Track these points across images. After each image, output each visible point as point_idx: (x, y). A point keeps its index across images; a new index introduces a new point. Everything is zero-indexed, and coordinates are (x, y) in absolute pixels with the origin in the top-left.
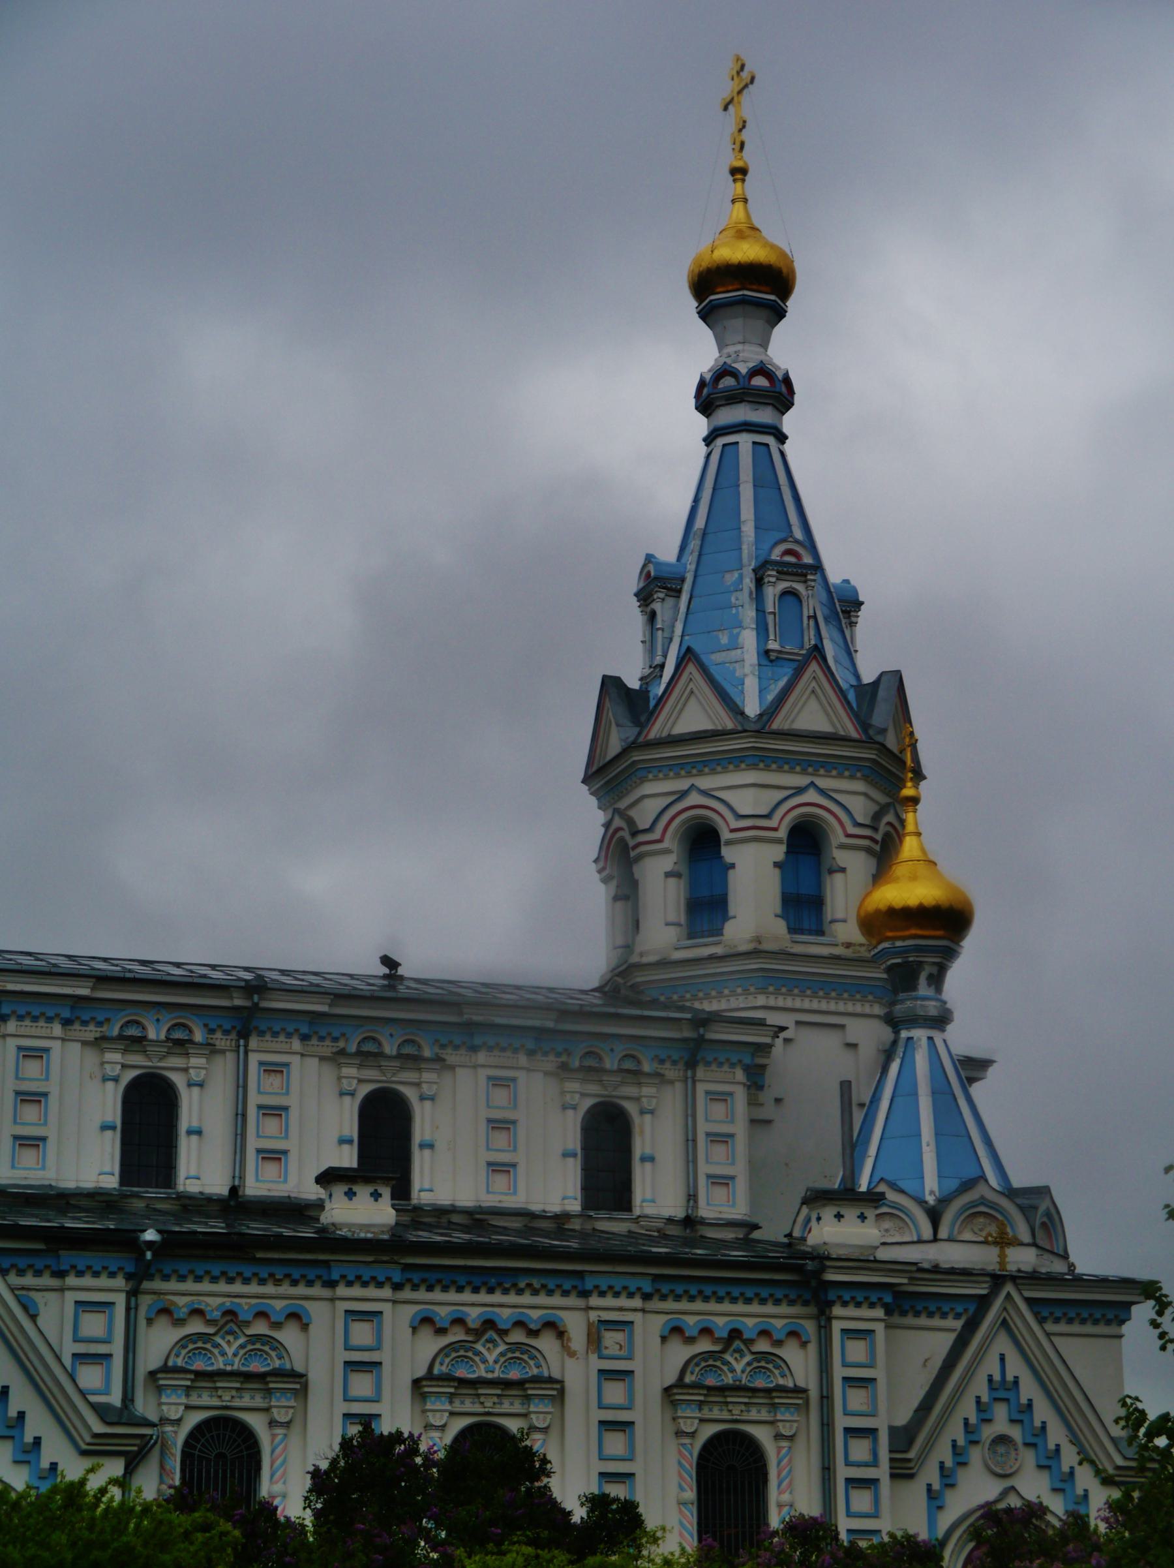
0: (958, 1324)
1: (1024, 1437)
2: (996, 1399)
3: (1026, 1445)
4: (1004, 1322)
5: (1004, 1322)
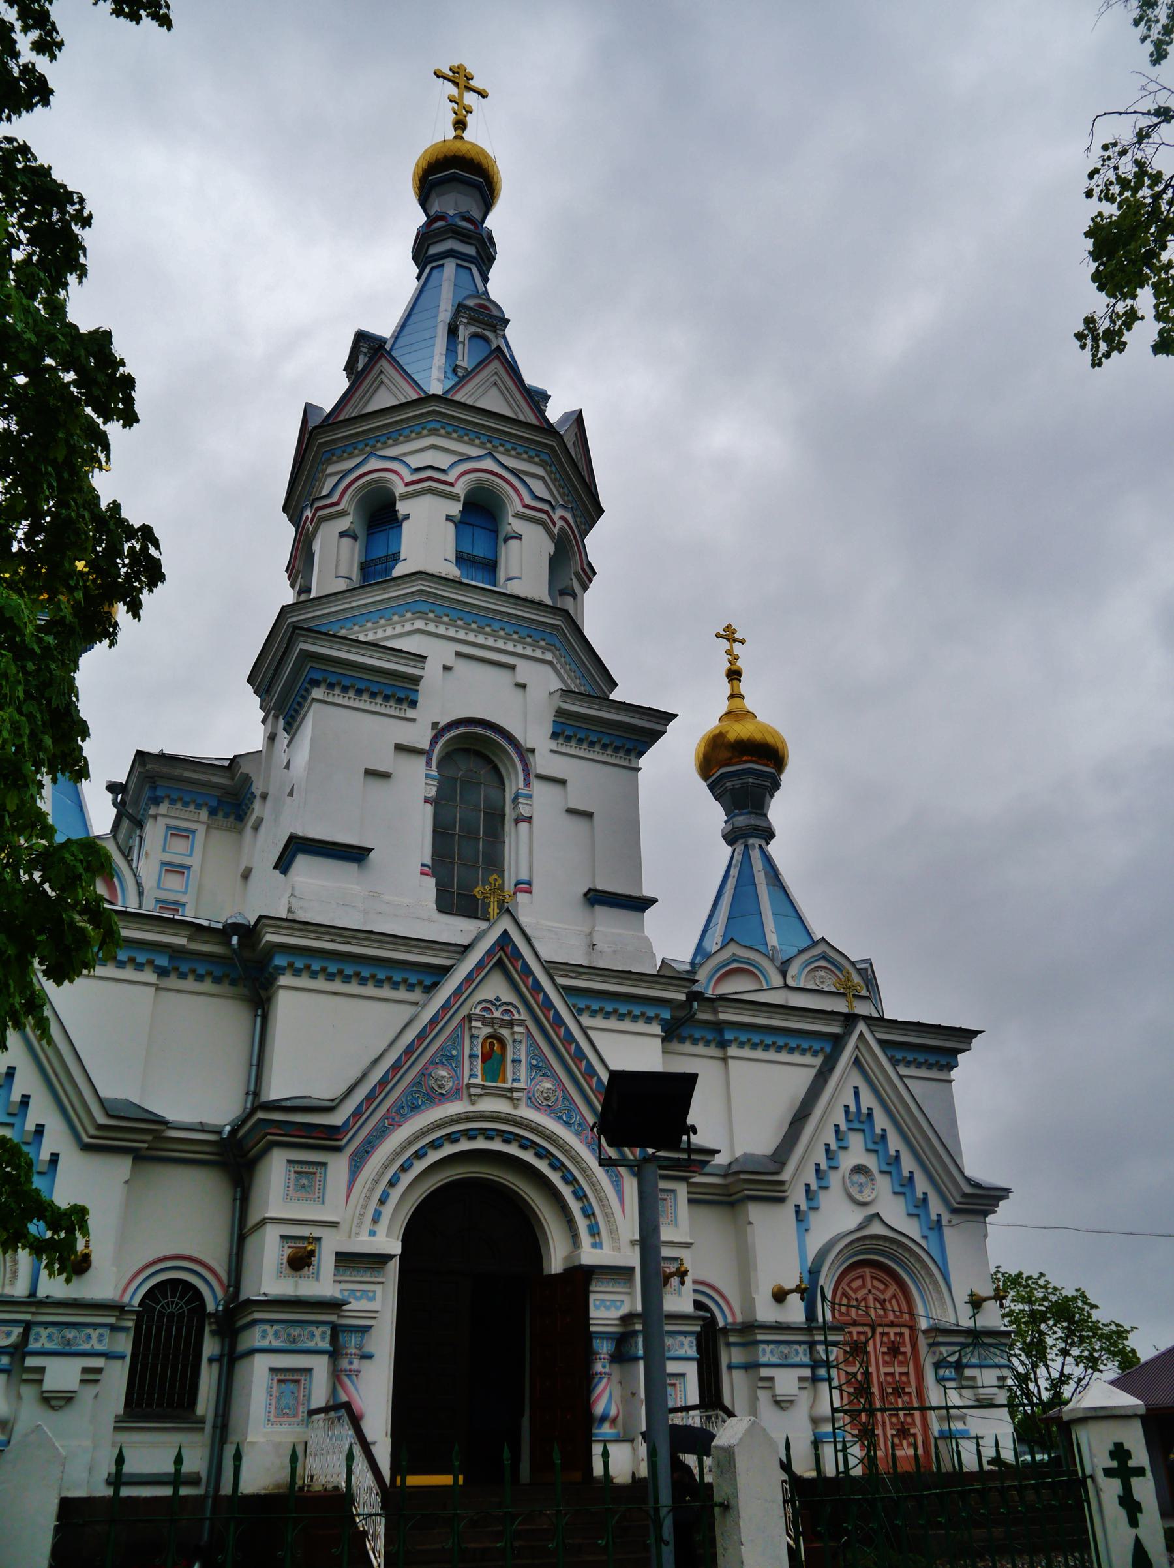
0: (818, 1061)
1: (879, 1166)
2: (850, 1129)
3: (882, 1172)
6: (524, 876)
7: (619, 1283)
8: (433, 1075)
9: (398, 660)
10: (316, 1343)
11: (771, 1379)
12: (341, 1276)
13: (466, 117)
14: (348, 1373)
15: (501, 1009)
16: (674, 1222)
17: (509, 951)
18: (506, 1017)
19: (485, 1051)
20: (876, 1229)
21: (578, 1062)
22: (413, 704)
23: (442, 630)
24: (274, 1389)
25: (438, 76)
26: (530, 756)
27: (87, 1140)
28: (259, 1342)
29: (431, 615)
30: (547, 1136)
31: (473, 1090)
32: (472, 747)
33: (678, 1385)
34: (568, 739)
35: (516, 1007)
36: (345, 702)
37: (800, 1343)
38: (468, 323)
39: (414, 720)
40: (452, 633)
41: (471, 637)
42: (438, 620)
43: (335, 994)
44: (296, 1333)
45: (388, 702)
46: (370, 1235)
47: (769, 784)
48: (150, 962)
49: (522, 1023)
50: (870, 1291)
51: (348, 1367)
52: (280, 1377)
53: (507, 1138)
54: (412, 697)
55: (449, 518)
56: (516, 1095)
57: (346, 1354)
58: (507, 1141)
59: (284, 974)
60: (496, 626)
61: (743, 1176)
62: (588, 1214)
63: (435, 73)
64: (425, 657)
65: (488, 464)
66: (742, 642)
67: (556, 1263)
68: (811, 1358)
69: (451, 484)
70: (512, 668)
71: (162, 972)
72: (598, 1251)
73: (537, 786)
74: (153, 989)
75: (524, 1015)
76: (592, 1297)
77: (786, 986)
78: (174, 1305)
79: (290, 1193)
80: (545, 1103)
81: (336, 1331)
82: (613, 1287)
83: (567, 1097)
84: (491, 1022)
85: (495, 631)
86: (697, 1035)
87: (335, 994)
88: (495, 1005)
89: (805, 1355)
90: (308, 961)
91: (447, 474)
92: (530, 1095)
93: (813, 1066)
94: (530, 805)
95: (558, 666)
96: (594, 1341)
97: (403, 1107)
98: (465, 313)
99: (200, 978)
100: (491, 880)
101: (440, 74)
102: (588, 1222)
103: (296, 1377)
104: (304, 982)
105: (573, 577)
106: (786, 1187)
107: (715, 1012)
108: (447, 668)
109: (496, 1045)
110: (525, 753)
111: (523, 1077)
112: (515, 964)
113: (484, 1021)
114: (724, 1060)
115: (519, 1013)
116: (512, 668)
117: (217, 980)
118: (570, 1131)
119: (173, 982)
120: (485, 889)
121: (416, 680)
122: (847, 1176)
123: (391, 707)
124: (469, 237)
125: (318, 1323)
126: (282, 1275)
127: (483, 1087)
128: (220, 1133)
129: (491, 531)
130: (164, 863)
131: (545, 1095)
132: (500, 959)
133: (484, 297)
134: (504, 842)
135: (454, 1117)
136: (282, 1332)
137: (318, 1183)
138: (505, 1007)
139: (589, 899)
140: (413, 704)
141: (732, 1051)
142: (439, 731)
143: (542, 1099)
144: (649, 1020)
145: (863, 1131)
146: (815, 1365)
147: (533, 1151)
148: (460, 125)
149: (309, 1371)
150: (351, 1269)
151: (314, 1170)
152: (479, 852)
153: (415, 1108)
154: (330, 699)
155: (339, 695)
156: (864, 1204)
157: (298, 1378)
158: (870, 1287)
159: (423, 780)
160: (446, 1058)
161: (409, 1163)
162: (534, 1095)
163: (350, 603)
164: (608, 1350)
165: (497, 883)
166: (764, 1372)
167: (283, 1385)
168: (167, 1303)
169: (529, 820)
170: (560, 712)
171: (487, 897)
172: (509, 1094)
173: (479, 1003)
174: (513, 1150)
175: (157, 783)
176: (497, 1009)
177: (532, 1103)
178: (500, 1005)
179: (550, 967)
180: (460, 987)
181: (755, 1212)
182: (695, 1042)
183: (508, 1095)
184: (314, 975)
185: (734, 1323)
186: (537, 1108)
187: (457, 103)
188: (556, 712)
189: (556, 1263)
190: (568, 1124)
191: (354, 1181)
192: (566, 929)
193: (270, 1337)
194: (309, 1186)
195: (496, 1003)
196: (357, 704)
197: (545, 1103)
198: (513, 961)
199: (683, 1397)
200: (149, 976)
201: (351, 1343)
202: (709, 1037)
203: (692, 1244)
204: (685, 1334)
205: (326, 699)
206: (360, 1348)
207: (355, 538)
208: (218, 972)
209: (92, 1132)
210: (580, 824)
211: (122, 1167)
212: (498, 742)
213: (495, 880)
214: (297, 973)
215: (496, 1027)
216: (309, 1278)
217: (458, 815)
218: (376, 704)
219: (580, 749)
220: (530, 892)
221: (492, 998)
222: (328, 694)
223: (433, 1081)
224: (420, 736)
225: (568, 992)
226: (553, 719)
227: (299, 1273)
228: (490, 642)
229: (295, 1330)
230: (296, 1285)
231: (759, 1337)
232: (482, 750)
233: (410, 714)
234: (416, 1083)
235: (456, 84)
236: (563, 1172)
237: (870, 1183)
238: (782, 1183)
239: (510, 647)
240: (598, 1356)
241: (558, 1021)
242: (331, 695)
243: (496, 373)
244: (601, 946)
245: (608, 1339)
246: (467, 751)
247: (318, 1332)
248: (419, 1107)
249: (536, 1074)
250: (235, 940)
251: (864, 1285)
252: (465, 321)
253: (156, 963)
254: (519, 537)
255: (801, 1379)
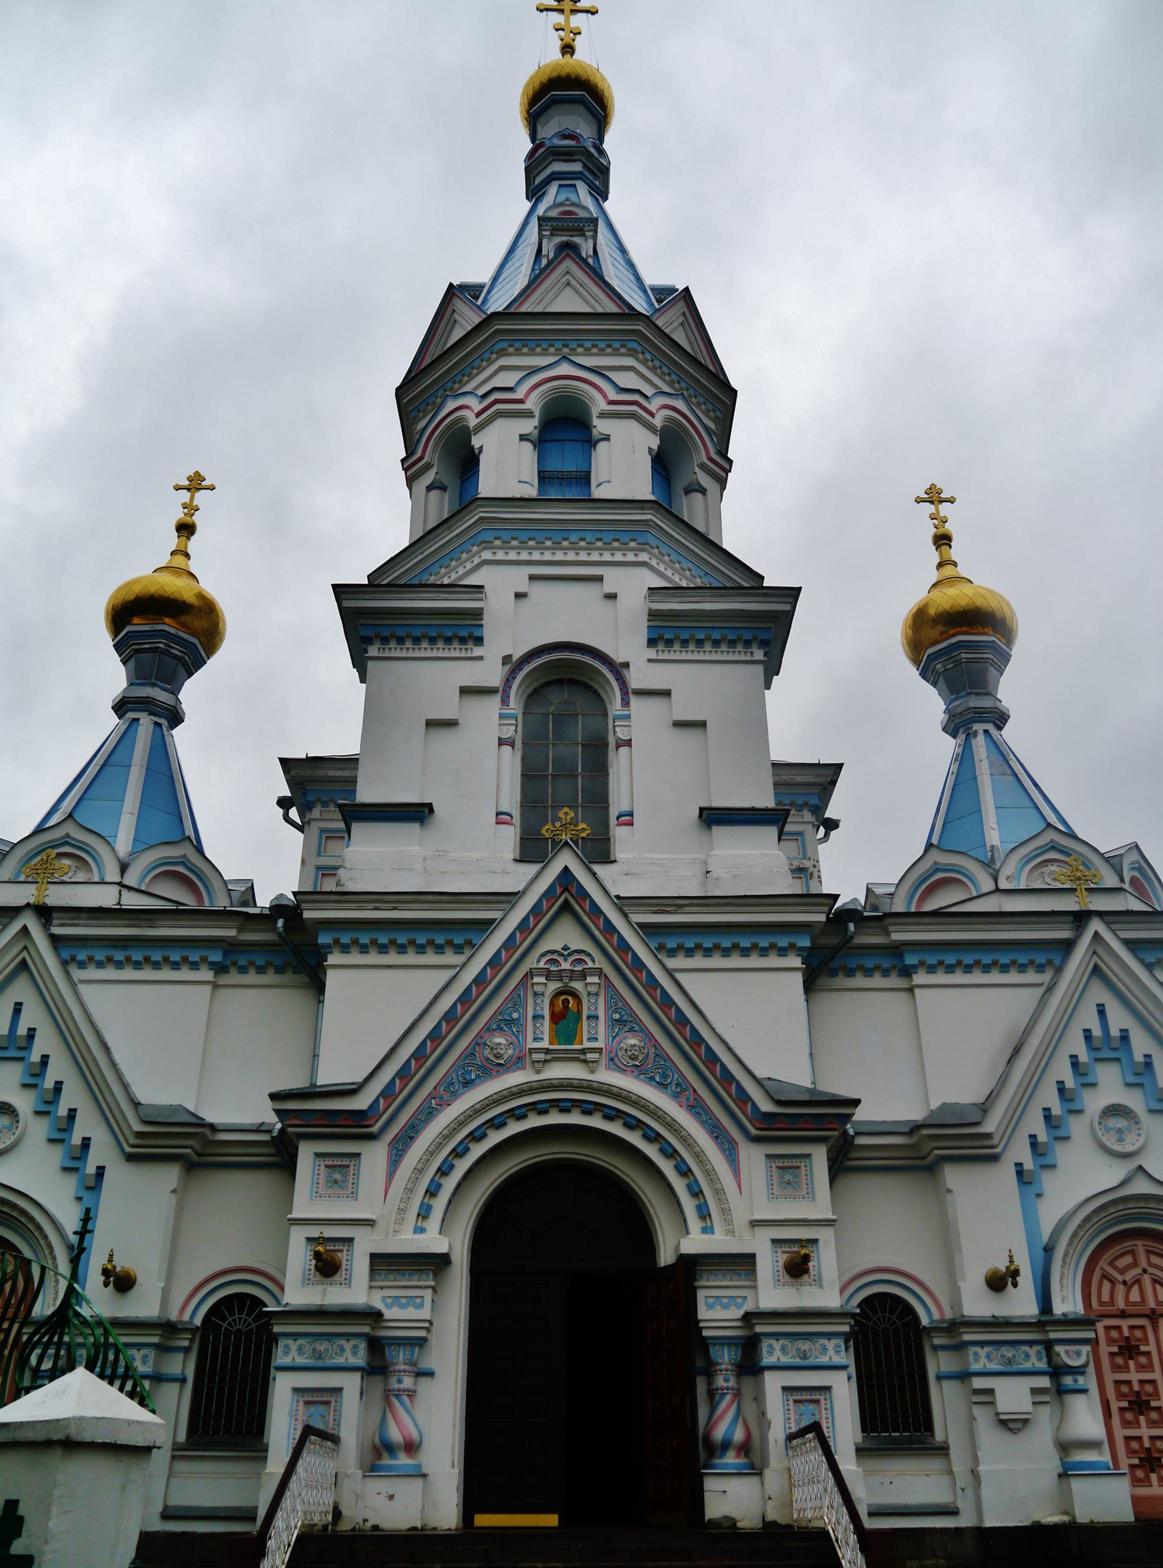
3: (1151, 1111)
4: (1096, 970)
5: (1096, 970)
6: (625, 807)
7: (739, 1275)
8: (489, 1043)
9: (451, 596)
10: (347, 1358)
11: (991, 1392)
12: (383, 1280)
13: (574, 40)
14: (396, 1393)
15: (571, 959)
16: (810, 1195)
17: (574, 891)
18: (579, 968)
19: (557, 1010)
20: (1141, 1187)
21: (666, 1010)
22: (479, 641)
23: (512, 556)
24: (300, 1413)
25: (541, 11)
26: (625, 671)
27: (128, 1149)
28: (281, 1358)
29: (498, 542)
30: (633, 1102)
31: (535, 1056)
32: (566, 677)
33: (823, 1402)
34: (669, 643)
35: (589, 955)
36: (404, 654)
37: (1030, 1343)
38: (552, 235)
39: (481, 658)
40: (524, 556)
41: (548, 556)
42: (506, 547)
43: (389, 967)
44: (322, 1348)
45: (451, 645)
46: (415, 1232)
47: (991, 656)
48: (204, 959)
49: (600, 972)
50: (1145, 1271)
51: (396, 1386)
52: (306, 1399)
53: (589, 1109)
54: (477, 633)
55: (523, 438)
56: (590, 1056)
57: (395, 1371)
58: (587, 1113)
59: (331, 952)
60: (574, 537)
61: (925, 1132)
62: (696, 1193)
63: (538, 9)
64: (482, 587)
65: (565, 369)
66: (951, 501)
67: (666, 1257)
68: (1050, 1363)
69: (521, 401)
70: (599, 579)
71: (220, 969)
72: (707, 1237)
73: (634, 700)
74: (209, 988)
75: (600, 962)
76: (701, 1295)
77: (997, 890)
78: (240, 1321)
79: (320, 1190)
80: (632, 1063)
81: (376, 1346)
82: (732, 1280)
83: (661, 1055)
84: (560, 975)
85: (574, 543)
86: (852, 964)
87: (389, 967)
88: (563, 955)
89: (1040, 1359)
90: (354, 935)
91: (515, 392)
92: (613, 1055)
93: (1040, 985)
94: (630, 726)
95: (654, 562)
96: (386, 1348)
97: (453, 1084)
98: (547, 225)
99: (261, 970)
100: (561, 814)
101: (543, 8)
102: (696, 1202)
103: (324, 1399)
104: (354, 958)
105: (697, 470)
106: (996, 1141)
107: (888, 934)
108: (519, 596)
109: (571, 1002)
110: (619, 669)
111: (601, 1035)
112: (583, 905)
113: (549, 975)
114: (911, 990)
115: (594, 961)
116: (599, 579)
117: (280, 970)
118: (667, 1094)
119: (234, 977)
120: (554, 826)
121: (478, 614)
122: (1097, 1120)
123: (455, 649)
124: (572, 154)
125: (348, 1336)
126: (310, 1282)
127: (547, 1051)
128: (270, 1132)
129: (584, 441)
130: (318, 868)
131: (630, 1053)
132: (566, 902)
133: (568, 203)
134: (608, 775)
135: (513, 1089)
136: (308, 1346)
137: (351, 1177)
138: (576, 956)
139: (704, 821)
140: (479, 641)
141: (920, 978)
142: (514, 666)
143: (628, 1059)
144: (783, 952)
145: (1118, 1060)
146: (1057, 1371)
147: (621, 1122)
148: (568, 49)
149: (339, 1391)
150: (395, 1272)
151: (348, 1163)
152: (578, 789)
153: (468, 1084)
154: (387, 654)
155: (395, 649)
156: (1126, 1156)
157: (329, 1399)
158: (1144, 1264)
159: (496, 719)
160: (506, 1023)
161: (462, 1147)
162: (617, 1055)
163: (422, 553)
164: (730, 1359)
165: (568, 817)
166: (978, 1383)
167: (312, 1408)
168: (234, 1320)
169: (628, 743)
170: (653, 615)
171: (558, 835)
172: (582, 1057)
173: (543, 955)
174: (596, 1122)
175: (307, 788)
176: (566, 960)
177: (613, 1063)
178: (569, 955)
179: (623, 903)
180: (512, 936)
181: (953, 1175)
182: (868, 973)
183: (579, 1057)
184: (364, 949)
185: (942, 1321)
186: (622, 1070)
187: (563, 30)
188: (649, 615)
189: (666, 1257)
190: (662, 1086)
191: (395, 1172)
192: (674, 859)
193: (293, 1353)
194: (343, 1181)
195: (566, 952)
196: (417, 654)
197: (632, 1063)
198: (581, 903)
199: (830, 1417)
200: (206, 974)
201: (399, 1358)
202: (886, 964)
203: (834, 1221)
204: (829, 1336)
205: (381, 655)
206: (414, 1364)
207: (443, 488)
208: (278, 961)
209: (132, 1140)
210: (690, 737)
211: (170, 1175)
212: (589, 664)
213: (566, 814)
214: (345, 949)
215: (566, 980)
216: (341, 1284)
217: (551, 754)
218: (438, 649)
219: (687, 652)
220: (632, 825)
221: (558, 947)
222: (384, 649)
223: (489, 1051)
224: (490, 673)
225: (647, 929)
226: (646, 624)
227: (329, 1279)
228: (571, 556)
229: (321, 1345)
230: (324, 1293)
231: (966, 1337)
232: (576, 677)
233: (477, 651)
234: (470, 1054)
235: (562, 11)
236: (661, 1143)
237: (1134, 1128)
238: (988, 1136)
239: (595, 557)
240: (718, 1367)
241: (638, 965)
242: (387, 650)
243: (568, 272)
244: (717, 871)
245: (729, 1345)
246: (559, 682)
247: (348, 1346)
248: (473, 1081)
249: (620, 1030)
250: (280, 923)
251: (1135, 1264)
252: (548, 233)
253: (210, 959)
254: (607, 438)
255: (1035, 1391)
